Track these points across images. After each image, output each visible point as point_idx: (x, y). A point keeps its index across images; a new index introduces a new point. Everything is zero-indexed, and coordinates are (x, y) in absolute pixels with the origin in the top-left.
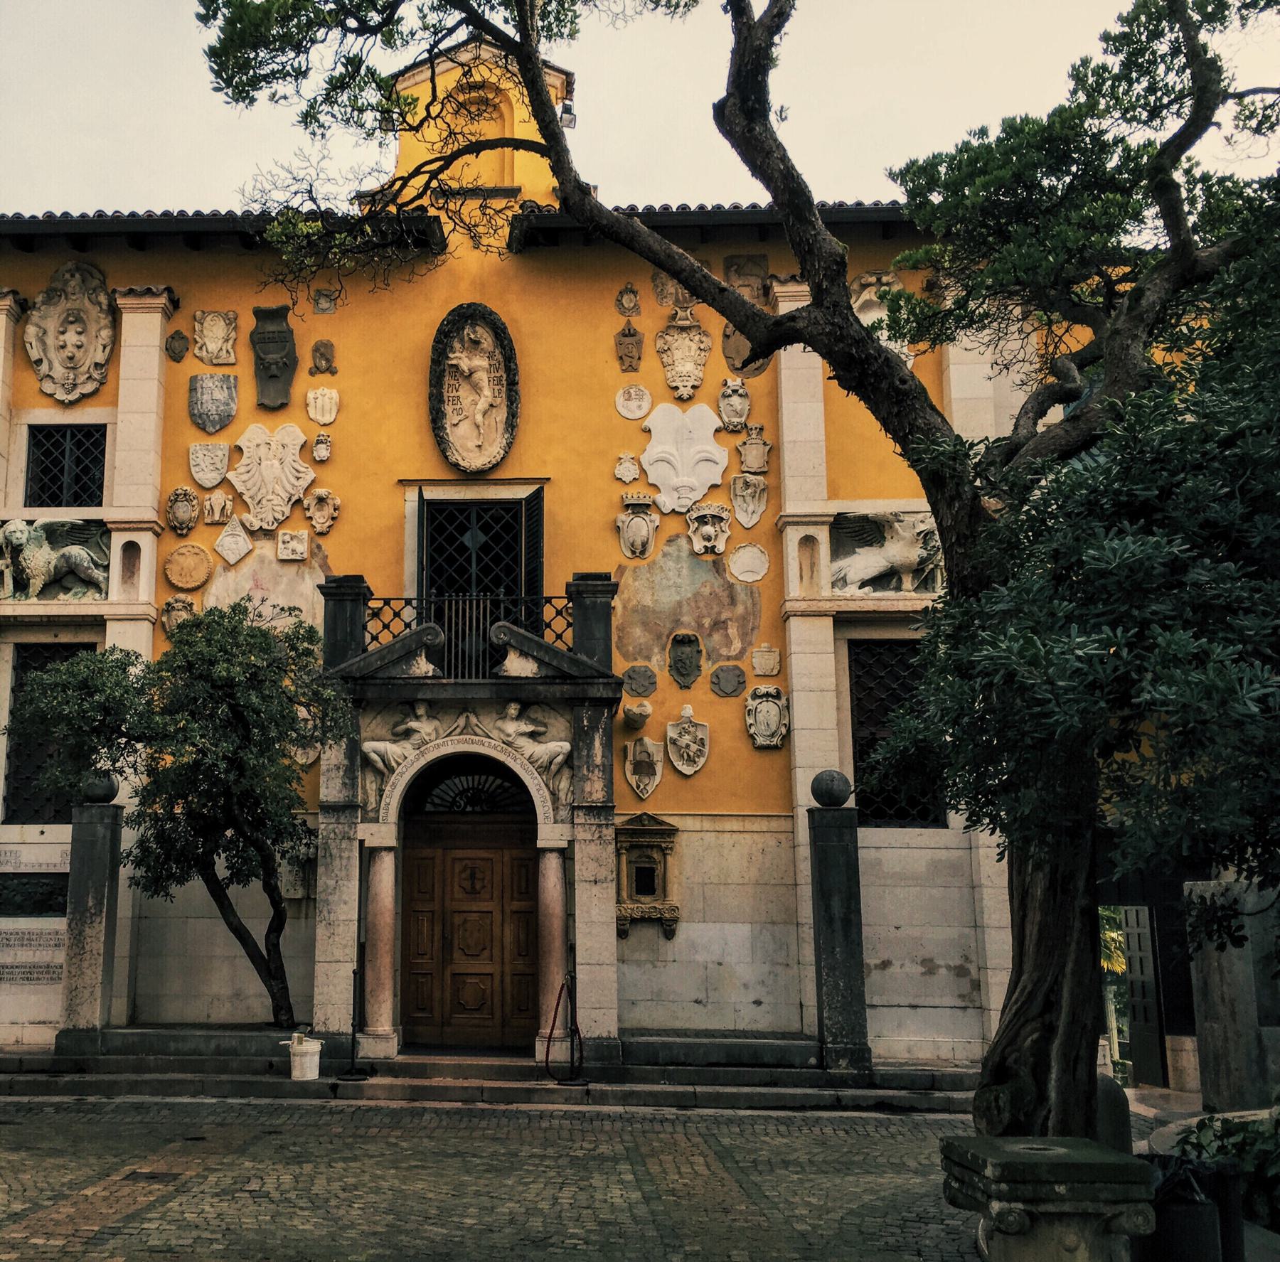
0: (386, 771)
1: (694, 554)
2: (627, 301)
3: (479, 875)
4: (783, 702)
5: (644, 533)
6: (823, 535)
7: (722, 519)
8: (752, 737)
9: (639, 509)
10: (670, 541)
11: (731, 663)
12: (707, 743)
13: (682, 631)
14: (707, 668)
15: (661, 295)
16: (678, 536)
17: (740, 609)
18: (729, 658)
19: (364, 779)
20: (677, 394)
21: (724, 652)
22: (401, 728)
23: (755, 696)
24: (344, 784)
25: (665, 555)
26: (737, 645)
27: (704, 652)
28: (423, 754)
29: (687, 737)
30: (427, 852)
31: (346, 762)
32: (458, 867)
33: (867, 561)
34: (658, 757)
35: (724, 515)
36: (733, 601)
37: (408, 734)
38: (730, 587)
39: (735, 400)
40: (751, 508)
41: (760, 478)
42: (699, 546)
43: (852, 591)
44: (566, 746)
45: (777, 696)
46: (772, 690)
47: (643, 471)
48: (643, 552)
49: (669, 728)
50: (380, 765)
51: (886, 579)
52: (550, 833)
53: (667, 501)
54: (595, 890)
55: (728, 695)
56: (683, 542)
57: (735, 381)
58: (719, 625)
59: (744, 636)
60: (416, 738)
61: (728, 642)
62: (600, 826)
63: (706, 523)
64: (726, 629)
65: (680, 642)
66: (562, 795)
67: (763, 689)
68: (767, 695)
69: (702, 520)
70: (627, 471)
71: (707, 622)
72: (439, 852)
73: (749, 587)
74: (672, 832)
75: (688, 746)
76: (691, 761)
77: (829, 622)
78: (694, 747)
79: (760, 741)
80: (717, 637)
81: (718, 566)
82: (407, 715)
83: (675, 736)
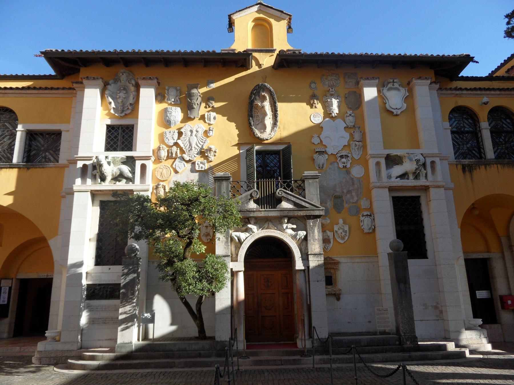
1: (339, 168)
2: (313, 86)
4: (372, 218)
5: (323, 161)
6: (383, 162)
7: (348, 156)
8: (363, 230)
9: (321, 153)
10: (331, 164)
13: (338, 194)
14: (346, 206)
16: (334, 162)
17: (356, 186)
18: (353, 203)
20: (331, 116)
21: (351, 201)
23: (363, 216)
26: (356, 198)
33: (397, 170)
34: (331, 237)
35: (349, 155)
36: (353, 184)
38: (352, 179)
39: (351, 117)
40: (357, 153)
41: (360, 143)
42: (341, 166)
45: (370, 216)
46: (369, 214)
47: (321, 141)
48: (322, 168)
51: (404, 176)
53: (330, 151)
56: (336, 164)
57: (350, 112)
58: (349, 192)
59: (357, 196)
65: (336, 197)
67: (365, 213)
68: (367, 215)
69: (342, 157)
70: (316, 141)
71: (345, 191)
73: (358, 179)
76: (343, 238)
77: (387, 190)
79: (366, 231)
80: (349, 196)
81: (348, 172)
83: (337, 230)
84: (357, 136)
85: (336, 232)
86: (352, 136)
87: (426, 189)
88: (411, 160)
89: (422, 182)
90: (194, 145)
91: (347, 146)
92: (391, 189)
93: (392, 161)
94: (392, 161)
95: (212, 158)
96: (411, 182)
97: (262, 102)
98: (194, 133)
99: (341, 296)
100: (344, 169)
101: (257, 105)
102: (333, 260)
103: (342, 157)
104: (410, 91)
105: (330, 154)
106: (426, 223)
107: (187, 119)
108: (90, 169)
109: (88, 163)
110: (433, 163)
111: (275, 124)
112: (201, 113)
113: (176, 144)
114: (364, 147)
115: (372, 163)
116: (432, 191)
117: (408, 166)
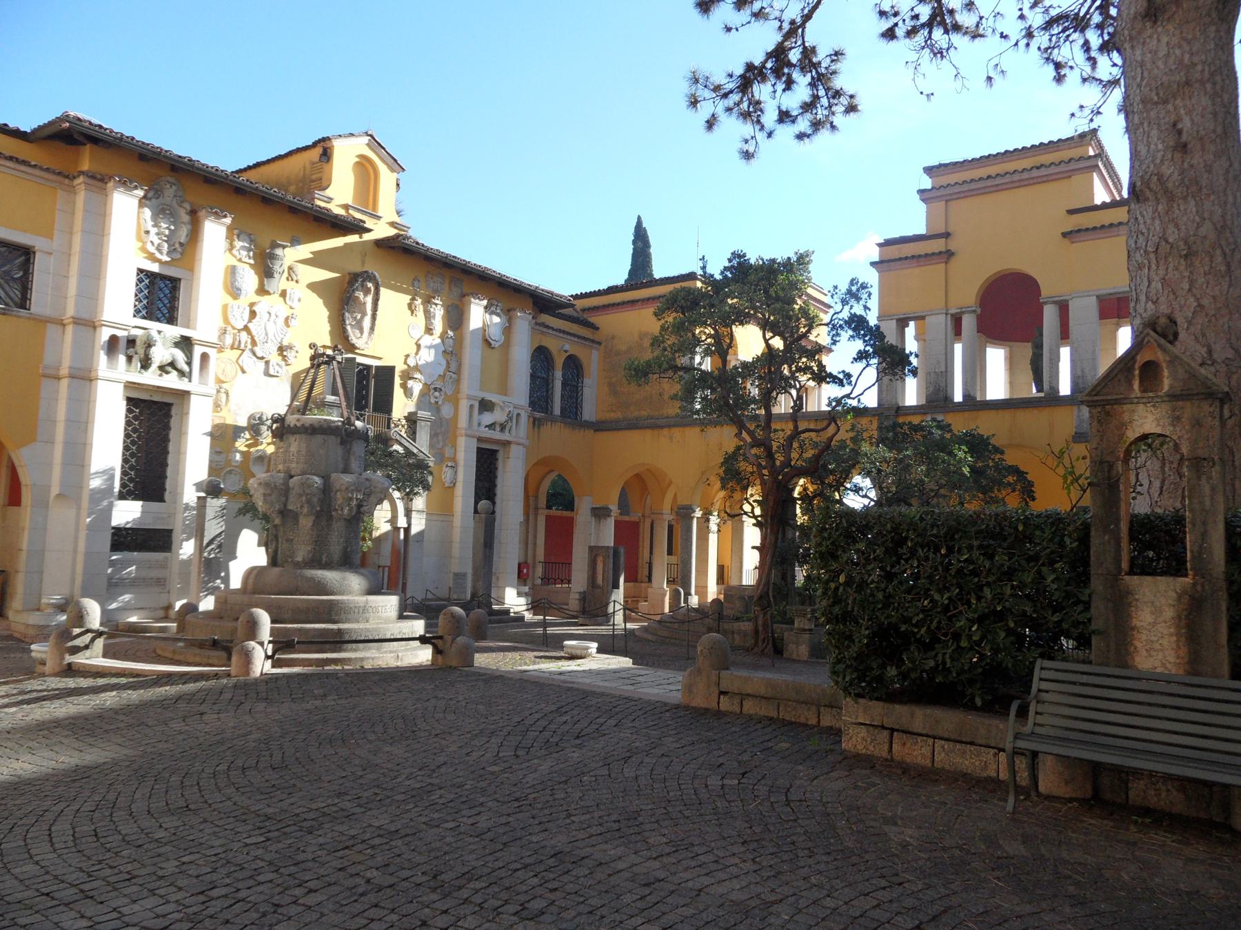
2: (416, 283)
15: (427, 286)
33: (488, 418)
42: (433, 401)
43: (482, 428)
51: (491, 426)
69: (435, 389)
84: (453, 367)
86: (448, 363)
87: (507, 444)
88: (502, 409)
89: (505, 437)
90: (271, 336)
91: (442, 377)
92: (480, 440)
93: (486, 406)
94: (486, 406)
95: (291, 360)
96: (496, 435)
97: (366, 294)
98: (273, 316)
101: (358, 298)
103: (435, 389)
104: (510, 320)
106: (499, 481)
107: (262, 291)
108: (122, 344)
109: (120, 333)
110: (518, 415)
111: (372, 329)
112: (281, 287)
113: (246, 328)
114: (458, 381)
115: (464, 405)
116: (513, 447)
117: (498, 416)
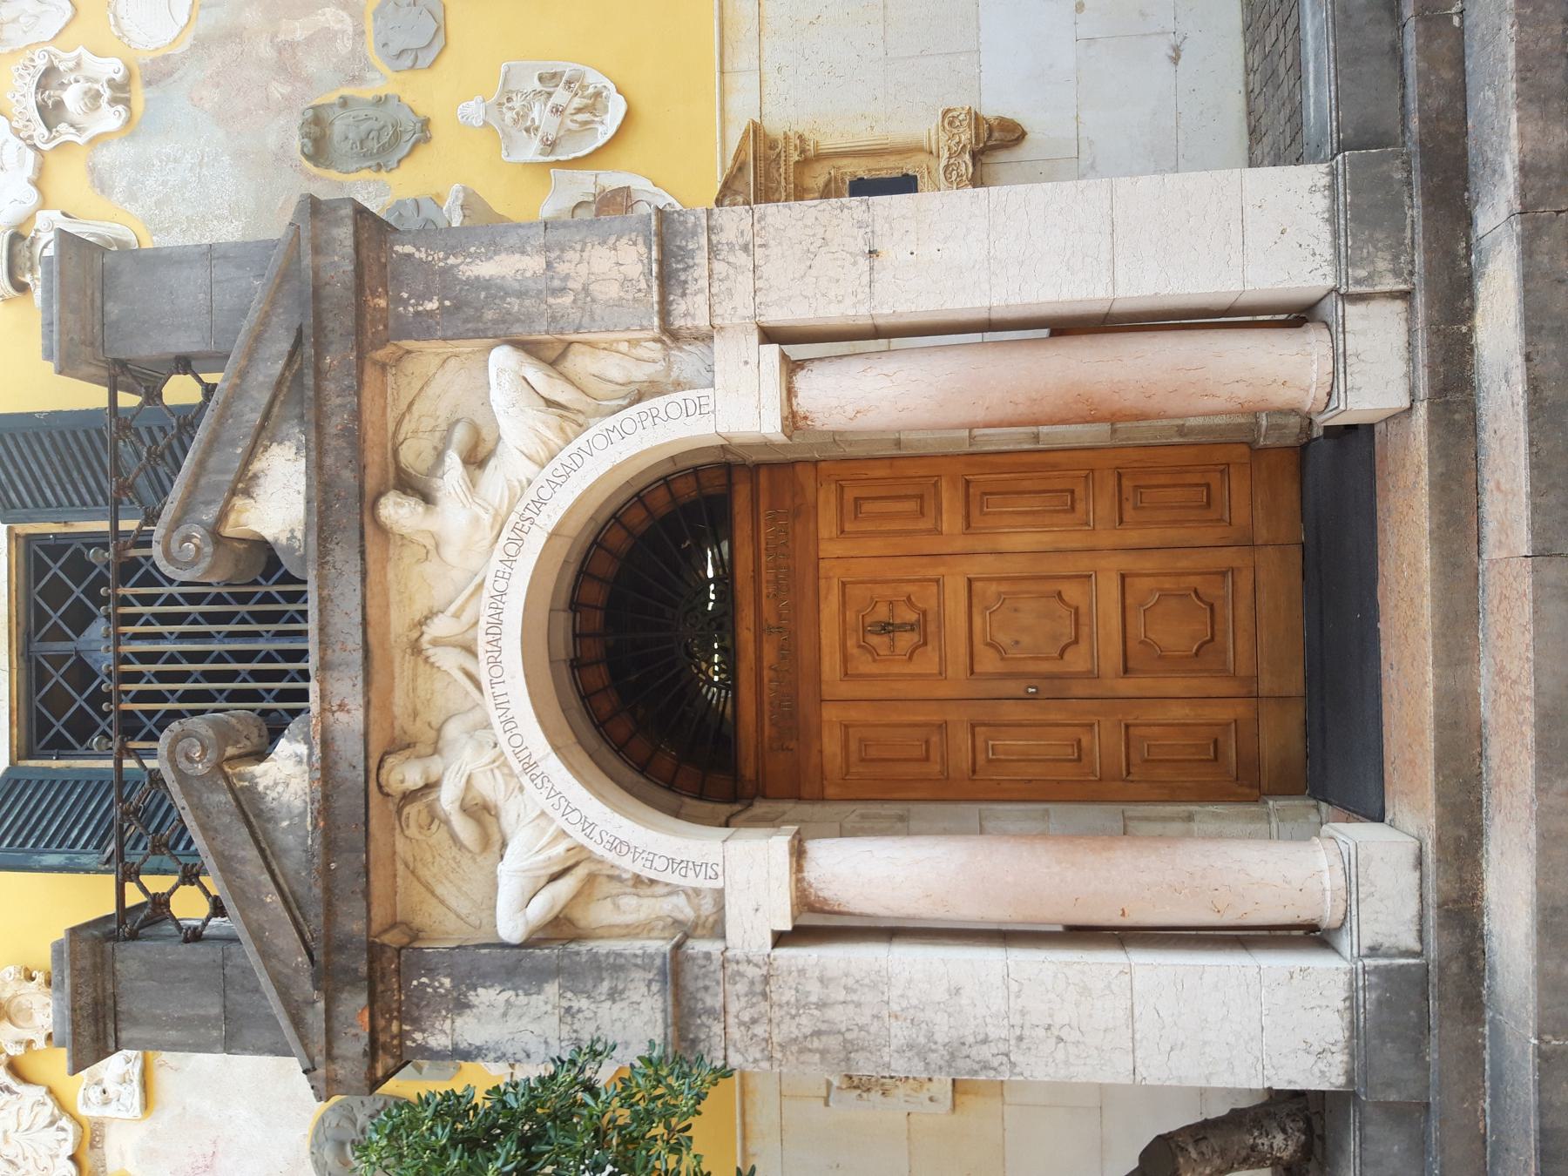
0: (581, 872)
3: (882, 613)
11: (369, 25)
12: (549, 67)
14: (381, 82)
16: (92, 170)
18: (360, 33)
19: (611, 932)
21: (344, 46)
22: (464, 829)
24: (614, 995)
25: (132, 197)
27: (347, 91)
28: (530, 766)
29: (535, 114)
30: (831, 745)
31: (552, 989)
32: (864, 665)
34: (585, 184)
35: (42, 64)
36: (232, 35)
37: (480, 811)
38: (201, 43)
42: (110, 119)
44: (503, 358)
49: (513, 159)
50: (565, 887)
52: (737, 404)
54: (893, 252)
55: (441, 30)
56: (105, 156)
60: (490, 788)
61: (328, 36)
62: (713, 250)
63: (59, 104)
64: (293, 45)
66: (641, 373)
71: (279, 90)
72: (830, 713)
74: (756, 131)
75: (557, 110)
78: (561, 96)
82: (433, 815)
83: (536, 144)
85: (551, 145)
99: (992, 109)
100: (139, 95)
102: (740, 168)
105: (32, 197)
